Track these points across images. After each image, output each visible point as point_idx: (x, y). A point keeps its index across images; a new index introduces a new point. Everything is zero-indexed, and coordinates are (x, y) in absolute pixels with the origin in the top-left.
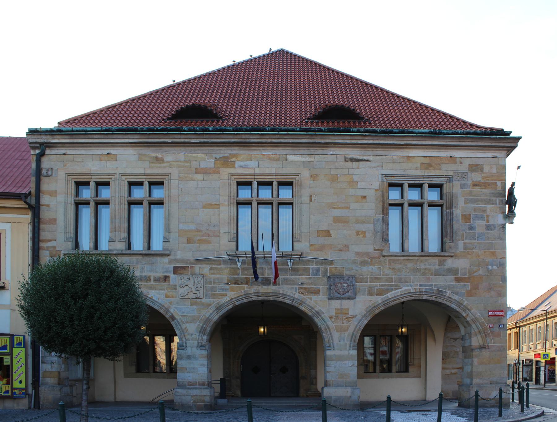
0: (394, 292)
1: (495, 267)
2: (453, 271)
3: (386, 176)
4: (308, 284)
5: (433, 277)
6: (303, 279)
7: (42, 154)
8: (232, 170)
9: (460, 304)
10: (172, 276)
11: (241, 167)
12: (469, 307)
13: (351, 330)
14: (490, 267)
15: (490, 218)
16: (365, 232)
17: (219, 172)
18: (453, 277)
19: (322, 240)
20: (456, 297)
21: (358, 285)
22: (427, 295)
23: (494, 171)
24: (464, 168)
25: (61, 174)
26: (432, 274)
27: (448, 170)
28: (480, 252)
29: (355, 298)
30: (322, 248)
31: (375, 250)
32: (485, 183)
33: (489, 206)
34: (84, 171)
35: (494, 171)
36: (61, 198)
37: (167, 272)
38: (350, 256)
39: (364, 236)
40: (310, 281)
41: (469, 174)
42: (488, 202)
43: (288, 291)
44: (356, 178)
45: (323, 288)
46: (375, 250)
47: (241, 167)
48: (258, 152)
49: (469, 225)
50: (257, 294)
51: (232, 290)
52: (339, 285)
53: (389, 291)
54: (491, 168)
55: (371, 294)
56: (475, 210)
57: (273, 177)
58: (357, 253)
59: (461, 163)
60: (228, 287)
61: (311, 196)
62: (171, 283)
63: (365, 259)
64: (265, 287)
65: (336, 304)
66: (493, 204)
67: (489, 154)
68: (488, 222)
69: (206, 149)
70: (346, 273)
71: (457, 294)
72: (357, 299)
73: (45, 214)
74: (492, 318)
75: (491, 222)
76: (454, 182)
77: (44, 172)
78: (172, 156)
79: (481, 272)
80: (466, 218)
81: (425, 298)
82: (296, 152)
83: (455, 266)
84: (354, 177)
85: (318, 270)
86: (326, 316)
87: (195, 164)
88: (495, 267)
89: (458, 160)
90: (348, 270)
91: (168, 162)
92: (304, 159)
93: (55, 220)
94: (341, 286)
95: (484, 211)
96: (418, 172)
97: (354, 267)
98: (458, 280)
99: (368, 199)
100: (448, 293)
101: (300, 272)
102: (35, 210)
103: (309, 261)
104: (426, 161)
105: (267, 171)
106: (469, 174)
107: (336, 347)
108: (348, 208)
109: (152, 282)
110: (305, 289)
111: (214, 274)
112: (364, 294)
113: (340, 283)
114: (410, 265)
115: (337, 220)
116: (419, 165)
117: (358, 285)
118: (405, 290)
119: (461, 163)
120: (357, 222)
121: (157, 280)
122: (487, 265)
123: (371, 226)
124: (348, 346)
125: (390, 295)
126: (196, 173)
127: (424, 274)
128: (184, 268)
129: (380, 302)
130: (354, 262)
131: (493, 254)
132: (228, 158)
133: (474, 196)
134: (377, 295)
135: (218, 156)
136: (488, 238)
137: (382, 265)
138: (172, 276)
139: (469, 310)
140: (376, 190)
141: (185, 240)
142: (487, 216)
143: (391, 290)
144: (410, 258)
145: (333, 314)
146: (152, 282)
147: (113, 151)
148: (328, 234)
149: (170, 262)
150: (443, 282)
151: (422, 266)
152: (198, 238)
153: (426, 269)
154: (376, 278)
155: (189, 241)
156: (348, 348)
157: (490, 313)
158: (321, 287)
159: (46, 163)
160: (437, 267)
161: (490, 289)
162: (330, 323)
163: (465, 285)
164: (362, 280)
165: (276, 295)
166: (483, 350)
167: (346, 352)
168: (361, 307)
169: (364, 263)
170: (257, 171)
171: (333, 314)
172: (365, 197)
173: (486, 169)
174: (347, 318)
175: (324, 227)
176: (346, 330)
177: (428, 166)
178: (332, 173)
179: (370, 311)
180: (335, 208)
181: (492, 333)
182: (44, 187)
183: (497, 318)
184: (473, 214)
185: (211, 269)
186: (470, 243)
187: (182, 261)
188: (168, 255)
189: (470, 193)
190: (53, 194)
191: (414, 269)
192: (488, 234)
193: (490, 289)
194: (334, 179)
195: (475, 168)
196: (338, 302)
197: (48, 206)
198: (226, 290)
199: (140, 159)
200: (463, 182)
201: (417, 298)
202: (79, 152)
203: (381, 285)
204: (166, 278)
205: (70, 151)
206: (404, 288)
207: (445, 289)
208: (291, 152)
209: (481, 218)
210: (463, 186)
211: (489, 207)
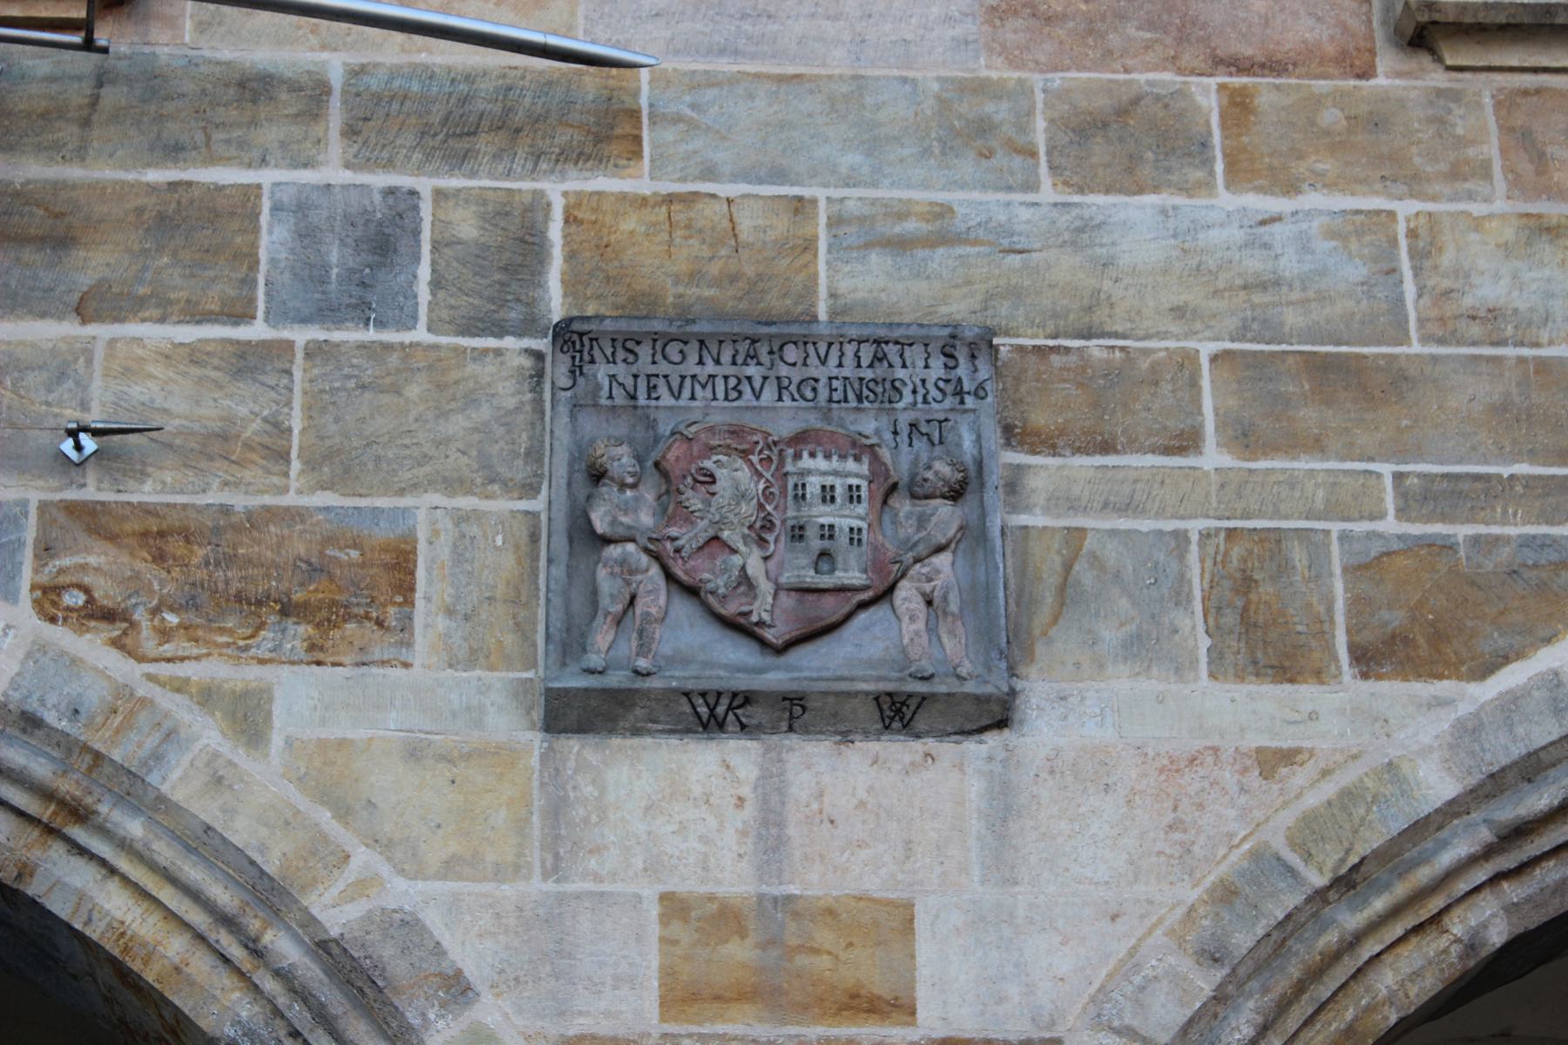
4: (216, 447)
21: (1051, 493)
29: (996, 715)
40: (245, 406)
45: (468, 533)
52: (734, 475)
55: (1265, 642)
65: (678, 808)
70: (850, 283)
72: (1044, 728)
85: (384, 237)
97: (973, 202)
101: (93, 264)
110: (159, 536)
112: (1144, 648)
113: (739, 441)
117: (1051, 493)
129: (1438, 785)
134: (1367, 660)
154: (1324, 384)
158: (427, 515)
164: (1115, 408)
196: (719, 767)
203: (1423, 498)
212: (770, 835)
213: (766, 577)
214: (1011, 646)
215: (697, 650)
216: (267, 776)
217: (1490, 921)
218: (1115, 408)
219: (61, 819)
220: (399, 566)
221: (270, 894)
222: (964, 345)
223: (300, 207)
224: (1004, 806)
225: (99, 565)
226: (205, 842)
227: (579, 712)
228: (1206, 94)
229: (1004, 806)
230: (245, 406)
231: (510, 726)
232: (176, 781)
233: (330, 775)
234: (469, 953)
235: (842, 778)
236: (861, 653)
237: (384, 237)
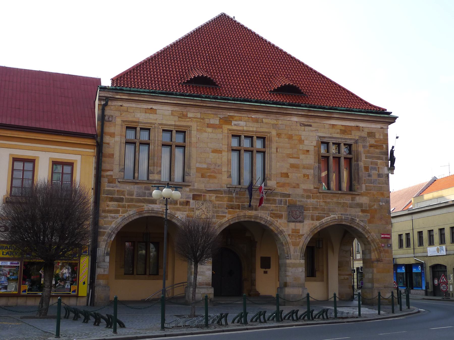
0: (326, 218)
1: (384, 204)
2: (360, 205)
3: (320, 137)
4: (275, 210)
6: (272, 206)
7: (106, 105)
8: (230, 127)
9: (364, 229)
10: (192, 201)
11: (235, 125)
12: (370, 231)
14: (381, 203)
15: (380, 170)
16: (308, 175)
17: (222, 128)
19: (283, 180)
20: (362, 224)
22: (345, 222)
23: (382, 137)
24: (364, 134)
25: (118, 121)
26: (347, 207)
27: (355, 135)
28: (375, 192)
30: (283, 185)
32: (376, 145)
33: (379, 161)
34: (134, 119)
35: (382, 137)
36: (117, 139)
37: (188, 198)
38: (299, 191)
39: (308, 178)
40: (277, 208)
41: (368, 138)
42: (379, 158)
43: (263, 215)
44: (303, 138)
45: (284, 214)
46: (315, 188)
47: (235, 125)
48: (246, 115)
49: (368, 173)
50: (245, 216)
51: (230, 213)
52: (294, 212)
53: (323, 217)
54: (380, 135)
55: (313, 220)
56: (371, 164)
57: (254, 133)
58: (304, 190)
59: (363, 131)
60: (227, 211)
62: (191, 207)
63: (308, 194)
64: (250, 212)
65: (292, 225)
66: (381, 160)
67: (379, 126)
69: (214, 111)
70: (298, 203)
71: (362, 221)
72: (305, 223)
73: (106, 150)
74: (383, 240)
75: (381, 172)
76: (359, 144)
77: (106, 118)
78: (192, 113)
79: (376, 206)
80: (367, 169)
81: (344, 223)
82: (268, 117)
83: (361, 202)
84: (302, 136)
85: (281, 201)
86: (286, 233)
87: (207, 121)
88: (384, 204)
90: (299, 201)
91: (190, 118)
92: (272, 123)
93: (113, 155)
94: (295, 213)
95: (376, 164)
96: (338, 136)
101: (271, 202)
102: (100, 147)
103: (276, 194)
104: (343, 128)
105: (251, 129)
106: (368, 138)
107: (292, 257)
108: (299, 158)
109: (178, 206)
110: (274, 214)
111: (218, 201)
112: (308, 219)
113: (295, 211)
114: (335, 200)
115: (293, 166)
116: (339, 131)
118: (333, 217)
119: (363, 131)
120: (304, 168)
121: (182, 204)
122: (379, 202)
123: (312, 171)
124: (299, 256)
125: (323, 220)
126: (208, 127)
127: (343, 206)
128: (200, 196)
129: (318, 225)
131: (382, 194)
132: (227, 117)
133: (370, 154)
135: (221, 116)
136: (379, 183)
137: (318, 199)
138: (192, 201)
139: (369, 233)
140: (315, 146)
141: (200, 175)
142: (378, 167)
143: (325, 218)
144: (335, 195)
145: (290, 233)
146: (178, 206)
147: (155, 107)
149: (191, 191)
150: (356, 212)
151: (342, 201)
152: (208, 174)
153: (344, 203)
154: (315, 209)
155: (203, 176)
156: (299, 258)
157: (382, 236)
159: (108, 112)
160: (351, 202)
162: (288, 239)
164: (308, 209)
165: (256, 217)
166: (379, 263)
167: (298, 261)
168: (307, 228)
169: (308, 197)
170: (245, 128)
171: (290, 233)
172: (308, 151)
173: (377, 136)
174: (299, 236)
175: (285, 171)
179: (312, 231)
180: (291, 158)
181: (384, 250)
182: (107, 129)
183: (386, 240)
184: (370, 166)
185: (216, 197)
186: (369, 186)
187: (198, 190)
188: (189, 186)
189: (368, 152)
190: (112, 135)
191: (337, 202)
192: (379, 180)
194: (290, 137)
195: (371, 134)
196: (293, 224)
197: (108, 144)
198: (226, 213)
199: (172, 114)
201: (339, 223)
202: (131, 105)
203: (319, 213)
204: (187, 203)
205: (126, 105)
206: (332, 216)
207: (356, 218)
208: (265, 117)
209: (374, 169)
210: (364, 147)
211: (379, 161)
212: (295, 227)
214: (304, 219)
215: (293, 219)
216: (278, 224)
218: (308, 209)
219: (271, 225)
221: (278, 228)
222: (302, 206)
223: (278, 199)
224: (303, 225)
226: (276, 226)
227: (288, 222)
229: (303, 225)
230: (277, 208)
231: (286, 222)
232: (275, 224)
233: (280, 224)
234: (285, 230)
235: (298, 224)
236: (299, 219)
237: (281, 201)
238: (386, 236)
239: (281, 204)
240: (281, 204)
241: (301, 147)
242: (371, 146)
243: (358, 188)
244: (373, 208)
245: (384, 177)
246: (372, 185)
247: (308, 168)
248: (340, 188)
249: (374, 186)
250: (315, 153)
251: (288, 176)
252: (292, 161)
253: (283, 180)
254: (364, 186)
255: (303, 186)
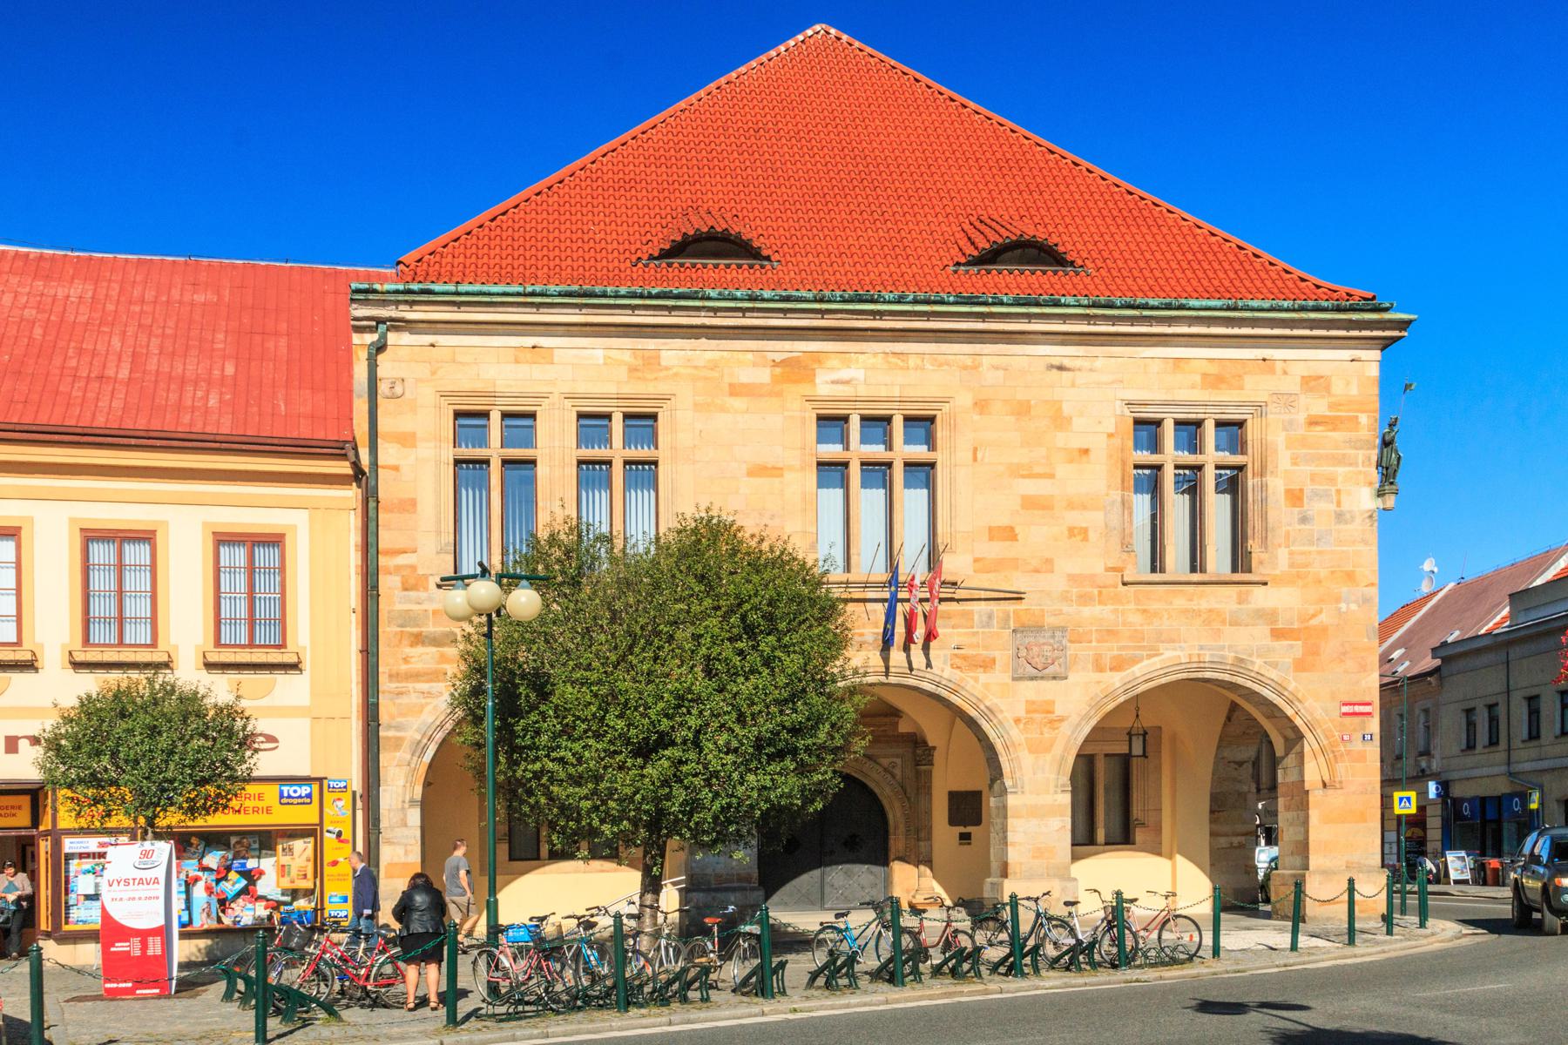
0: (1146, 662)
1: (1353, 607)
2: (1268, 616)
4: (972, 646)
5: (1227, 629)
13: (1058, 749)
14: (1343, 606)
15: (1344, 497)
16: (1085, 531)
18: (1266, 630)
20: (1273, 674)
23: (1354, 391)
24: (1291, 385)
26: (1223, 622)
30: (998, 565)
31: (1108, 569)
33: (1341, 470)
35: (1354, 391)
38: (1056, 583)
39: (1085, 539)
40: (974, 640)
42: (1341, 460)
44: (1067, 409)
45: (1003, 656)
46: (1108, 569)
53: (1135, 661)
54: (1348, 384)
56: (1312, 480)
58: (1073, 578)
59: (1285, 373)
61: (975, 450)
63: (1086, 590)
65: (1029, 690)
68: (1339, 504)
70: (1050, 620)
71: (1275, 665)
72: (1072, 677)
75: (1346, 506)
81: (1208, 675)
85: (990, 617)
89: (1279, 365)
95: (1332, 480)
97: (1065, 609)
98: (1277, 634)
99: (1092, 455)
100: (1258, 664)
104: (1213, 369)
107: (1027, 788)
108: (1052, 476)
110: (965, 658)
115: (1030, 503)
116: (1198, 378)
117: (1072, 649)
119: (1285, 373)
120: (1071, 506)
127: (1207, 622)
130: (1065, 597)
140: (1110, 435)
143: (1141, 660)
145: (1022, 714)
148: (1009, 534)
151: (1204, 605)
153: (1210, 611)
156: (1052, 789)
157: (1345, 709)
158: (997, 654)
160: (1235, 607)
161: (1344, 654)
163: (1292, 646)
168: (1079, 700)
169: (1084, 599)
171: (1022, 714)
172: (1086, 451)
173: (1338, 388)
174: (1051, 722)
175: (1004, 521)
176: (1048, 749)
177: (1214, 381)
178: (1019, 397)
180: (1023, 477)
184: (1308, 488)
186: (1302, 553)
193: (1344, 654)
194: (1022, 410)
195: (1313, 383)
200: (1287, 417)
203: (1120, 648)
206: (1168, 654)
210: (1288, 426)
211: (1341, 470)
213: (1039, 662)
215: (1031, 671)
217: (1122, 699)
220: (994, 661)
222: (1063, 629)
225: (958, 662)
228: (1096, 591)
230: (974, 640)
233: (986, 686)
236: (1051, 670)
238: (1358, 709)
239: (988, 625)
240: (988, 625)
241: (1061, 439)
242: (1313, 422)
243: (1261, 563)
244: (1313, 622)
245: (1358, 520)
246: (1314, 548)
247: (1084, 507)
248: (1196, 561)
249: (1320, 553)
250: (1110, 456)
251: (1014, 538)
252: (1031, 487)
253: (995, 550)
254: (1283, 555)
255: (1066, 566)
